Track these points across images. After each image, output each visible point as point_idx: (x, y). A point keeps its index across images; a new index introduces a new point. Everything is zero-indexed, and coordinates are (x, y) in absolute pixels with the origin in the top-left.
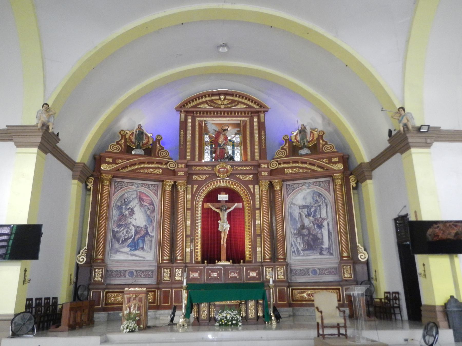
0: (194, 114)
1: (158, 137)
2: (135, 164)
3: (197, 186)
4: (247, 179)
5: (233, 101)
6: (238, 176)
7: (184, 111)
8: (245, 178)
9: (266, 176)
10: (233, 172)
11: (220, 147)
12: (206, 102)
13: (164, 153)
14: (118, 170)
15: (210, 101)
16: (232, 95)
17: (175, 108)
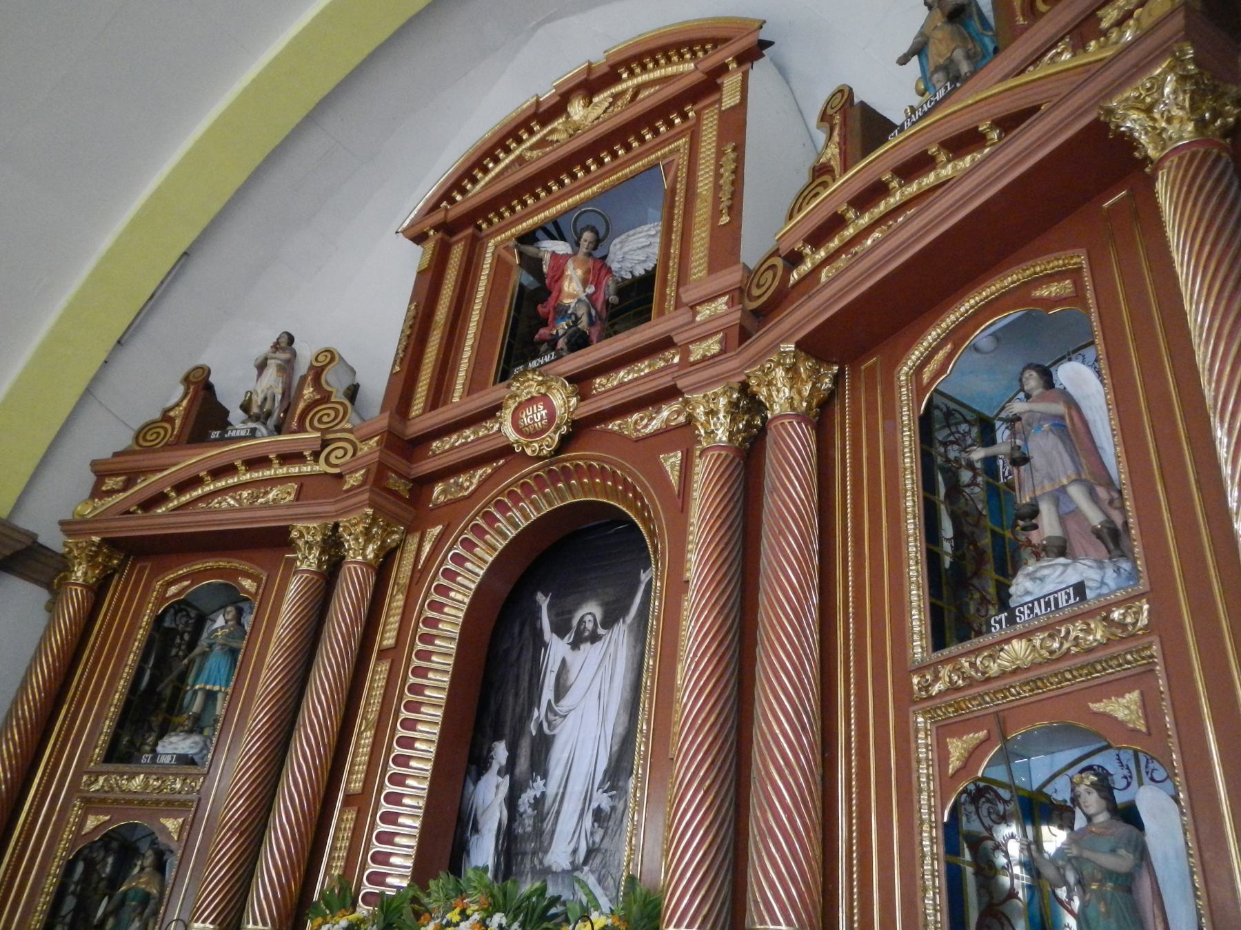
0: (479, 228)
1: (321, 358)
2: (196, 481)
3: (441, 527)
4: (655, 425)
5: (616, 97)
6: (614, 426)
7: (437, 228)
8: (646, 426)
9: (714, 356)
10: (588, 408)
11: (563, 319)
12: (520, 160)
13: (328, 415)
14: (128, 512)
15: (532, 148)
16: (610, 77)
17: (403, 232)
